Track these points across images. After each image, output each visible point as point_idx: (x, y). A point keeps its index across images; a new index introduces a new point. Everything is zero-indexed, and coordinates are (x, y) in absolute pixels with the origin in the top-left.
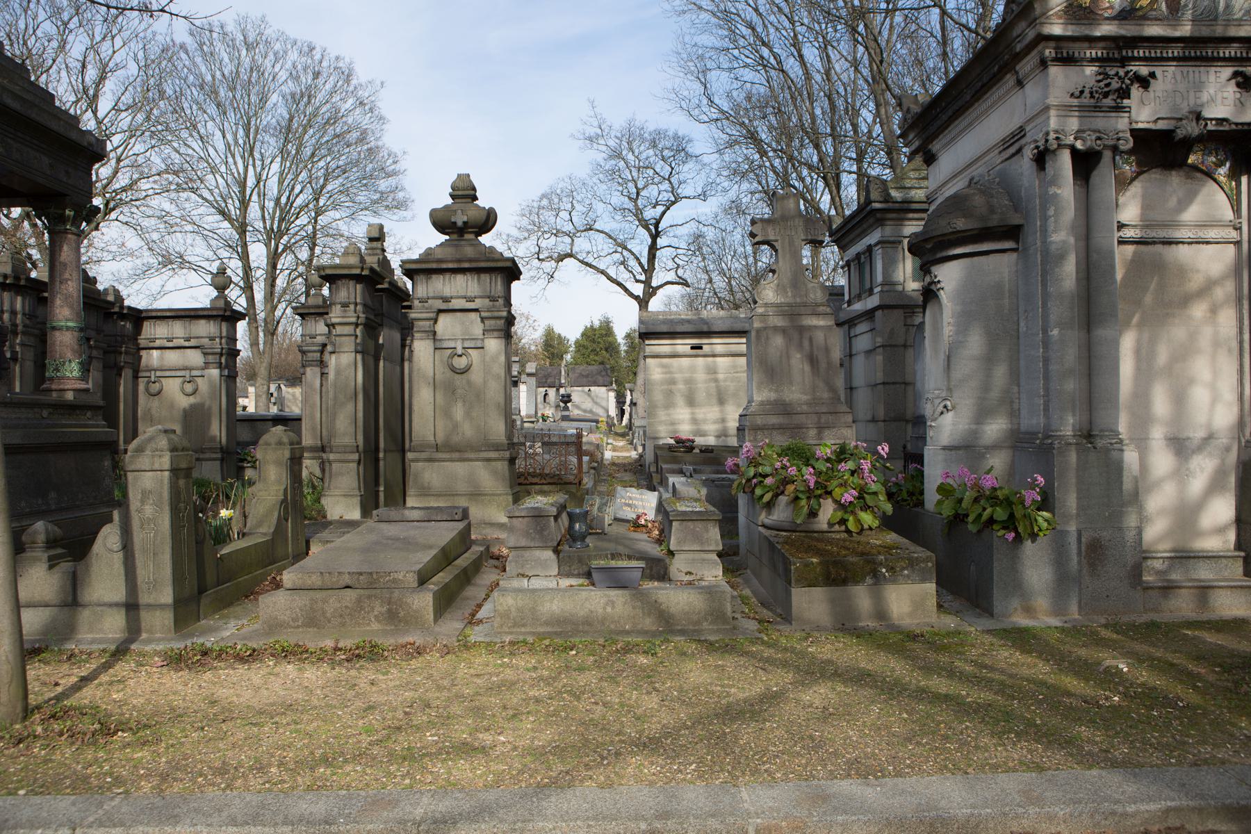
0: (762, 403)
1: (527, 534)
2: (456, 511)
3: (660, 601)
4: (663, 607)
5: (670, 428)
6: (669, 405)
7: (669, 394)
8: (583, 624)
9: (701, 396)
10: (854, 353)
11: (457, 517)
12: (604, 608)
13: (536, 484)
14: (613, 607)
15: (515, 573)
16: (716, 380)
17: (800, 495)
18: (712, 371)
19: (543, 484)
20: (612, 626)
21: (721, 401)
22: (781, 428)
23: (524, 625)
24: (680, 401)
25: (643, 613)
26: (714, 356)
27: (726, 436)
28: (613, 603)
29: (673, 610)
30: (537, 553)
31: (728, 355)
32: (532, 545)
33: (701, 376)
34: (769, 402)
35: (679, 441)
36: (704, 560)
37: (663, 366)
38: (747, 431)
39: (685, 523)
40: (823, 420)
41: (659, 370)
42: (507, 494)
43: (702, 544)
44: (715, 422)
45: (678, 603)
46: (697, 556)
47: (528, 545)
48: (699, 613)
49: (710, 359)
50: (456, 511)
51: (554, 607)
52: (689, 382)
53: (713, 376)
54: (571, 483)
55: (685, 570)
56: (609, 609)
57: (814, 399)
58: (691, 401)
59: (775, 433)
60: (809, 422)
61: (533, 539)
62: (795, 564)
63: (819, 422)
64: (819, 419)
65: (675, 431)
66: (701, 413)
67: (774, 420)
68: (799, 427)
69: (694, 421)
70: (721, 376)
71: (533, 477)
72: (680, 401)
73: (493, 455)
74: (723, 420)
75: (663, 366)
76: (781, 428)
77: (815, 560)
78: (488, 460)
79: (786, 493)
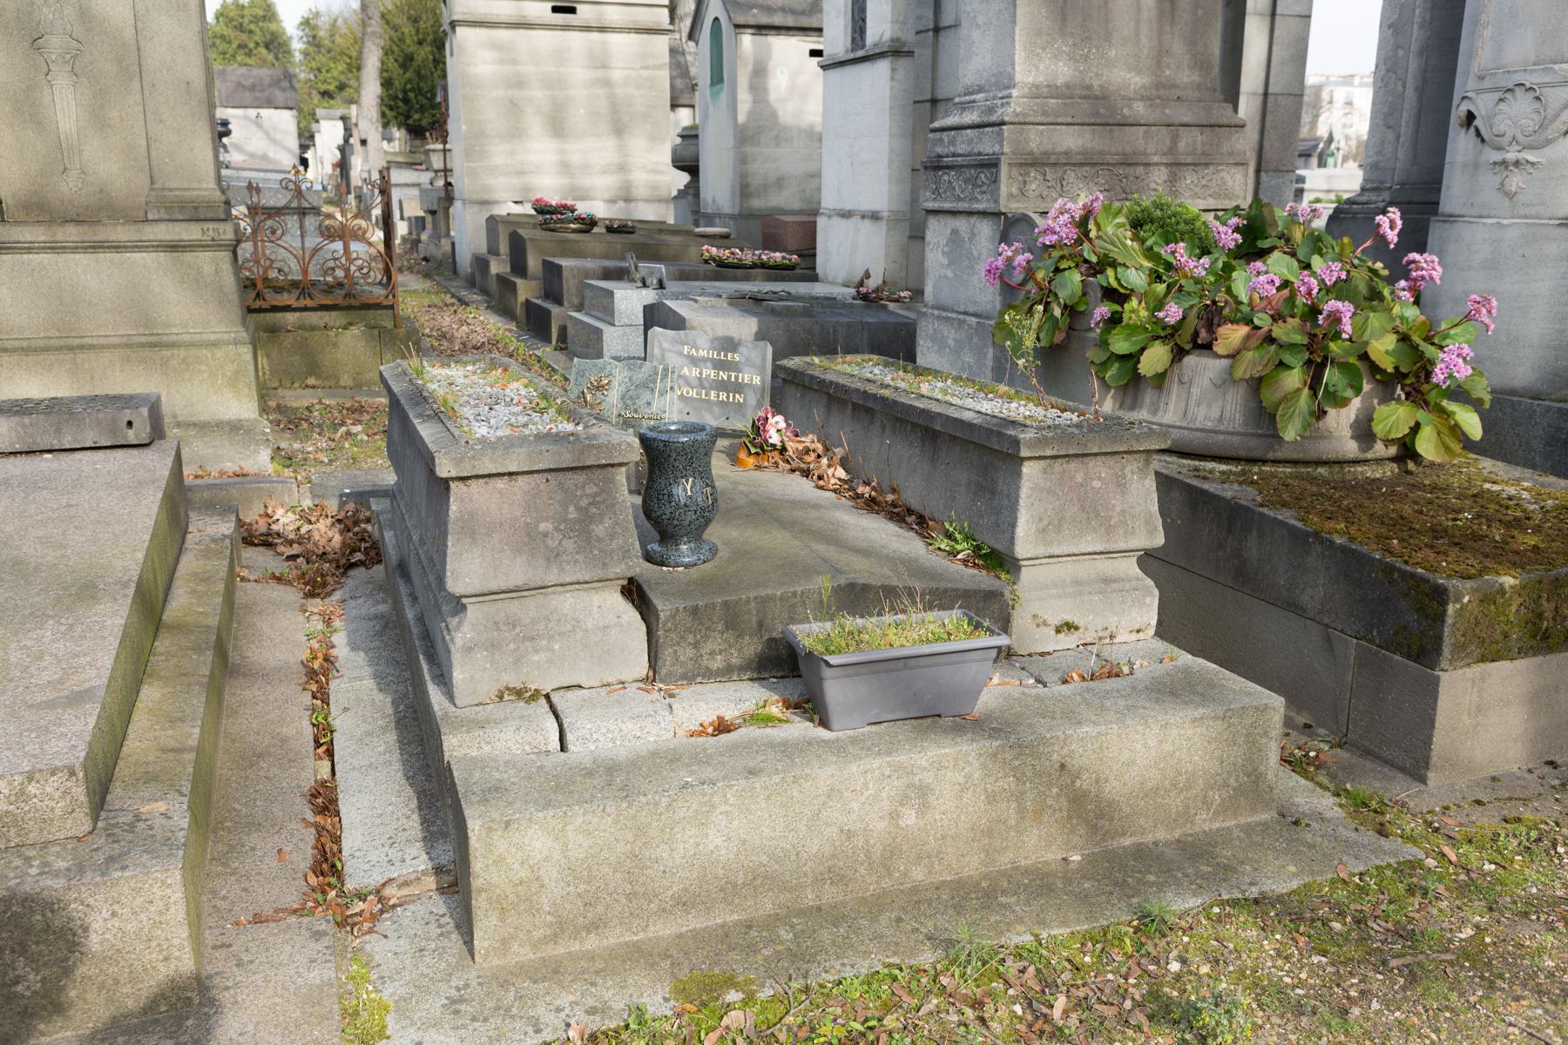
0: (1035, 93)
1: (530, 541)
2: (127, 415)
3: (1074, 763)
4: (1083, 783)
5: (515, 181)
6: (516, 133)
7: (513, 108)
8: (818, 881)
9: (578, 116)
10: (943, 24)
11: (131, 436)
12: (894, 816)
13: (287, 309)
14: (924, 808)
15: (488, 688)
16: (607, 83)
17: (1287, 358)
18: (601, 62)
19: (305, 309)
20: (918, 874)
21: (619, 129)
22: (1088, 163)
23: (594, 926)
24: (535, 124)
25: (1021, 811)
26: (602, 29)
27: (628, 200)
28: (923, 791)
29: (1112, 789)
30: (567, 603)
31: (629, 30)
32: (552, 578)
33: (578, 73)
34: (1054, 91)
35: (543, 209)
36: (1107, 581)
37: (497, 47)
38: (1004, 169)
39: (1058, 466)
40: (1182, 145)
41: (487, 55)
42: (236, 342)
43: (1110, 530)
44: (604, 171)
45: (1131, 763)
46: (1086, 568)
47: (536, 576)
48: (1189, 786)
49: (595, 36)
50: (127, 415)
51: (714, 840)
52: (554, 84)
53: (600, 73)
54: (378, 306)
55: (1056, 620)
56: (909, 818)
57: (1158, 86)
58: (557, 126)
59: (1071, 176)
60: (1151, 148)
61: (554, 556)
62: (1458, 599)
63: (1172, 150)
64: (1175, 139)
65: (526, 189)
66: (577, 150)
67: (1071, 140)
68: (1128, 162)
69: (565, 167)
70: (616, 75)
71: (279, 290)
72: (535, 124)
73: (192, 232)
74: (623, 168)
75: (497, 47)
76: (1088, 163)
77: (1508, 581)
78: (174, 247)
79: (1219, 348)
